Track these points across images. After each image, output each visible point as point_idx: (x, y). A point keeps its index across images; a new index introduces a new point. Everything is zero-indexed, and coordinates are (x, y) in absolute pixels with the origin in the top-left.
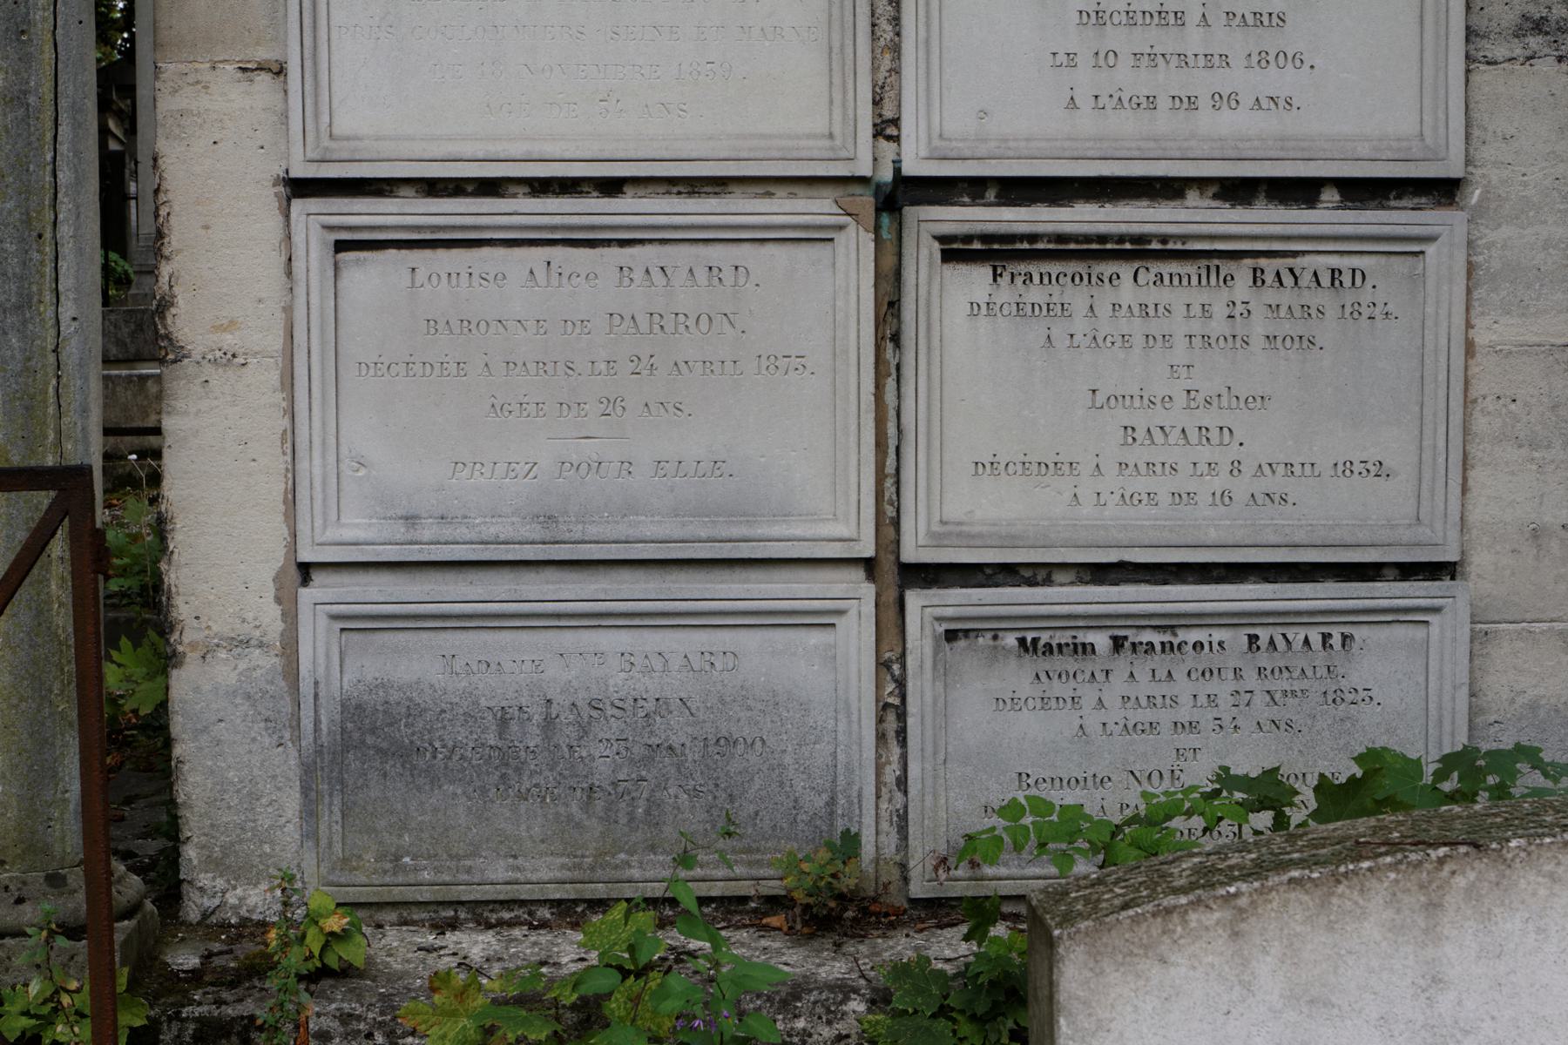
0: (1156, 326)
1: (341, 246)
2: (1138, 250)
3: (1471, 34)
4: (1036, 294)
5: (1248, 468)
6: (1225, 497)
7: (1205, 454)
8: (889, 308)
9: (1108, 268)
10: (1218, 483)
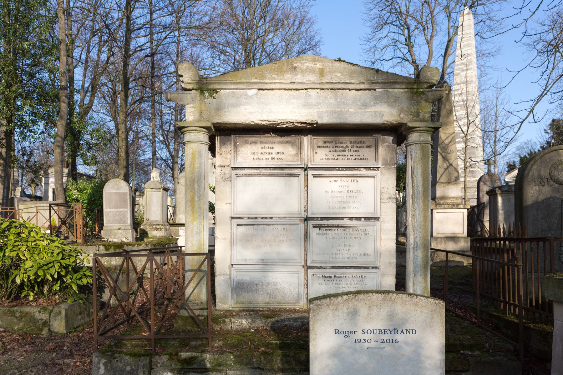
0: (340, 236)
1: (238, 225)
2: (338, 226)
3: (381, 199)
4: (325, 232)
5: (352, 254)
6: (349, 258)
7: (346, 252)
8: (306, 233)
9: (334, 229)
10: (348, 256)
